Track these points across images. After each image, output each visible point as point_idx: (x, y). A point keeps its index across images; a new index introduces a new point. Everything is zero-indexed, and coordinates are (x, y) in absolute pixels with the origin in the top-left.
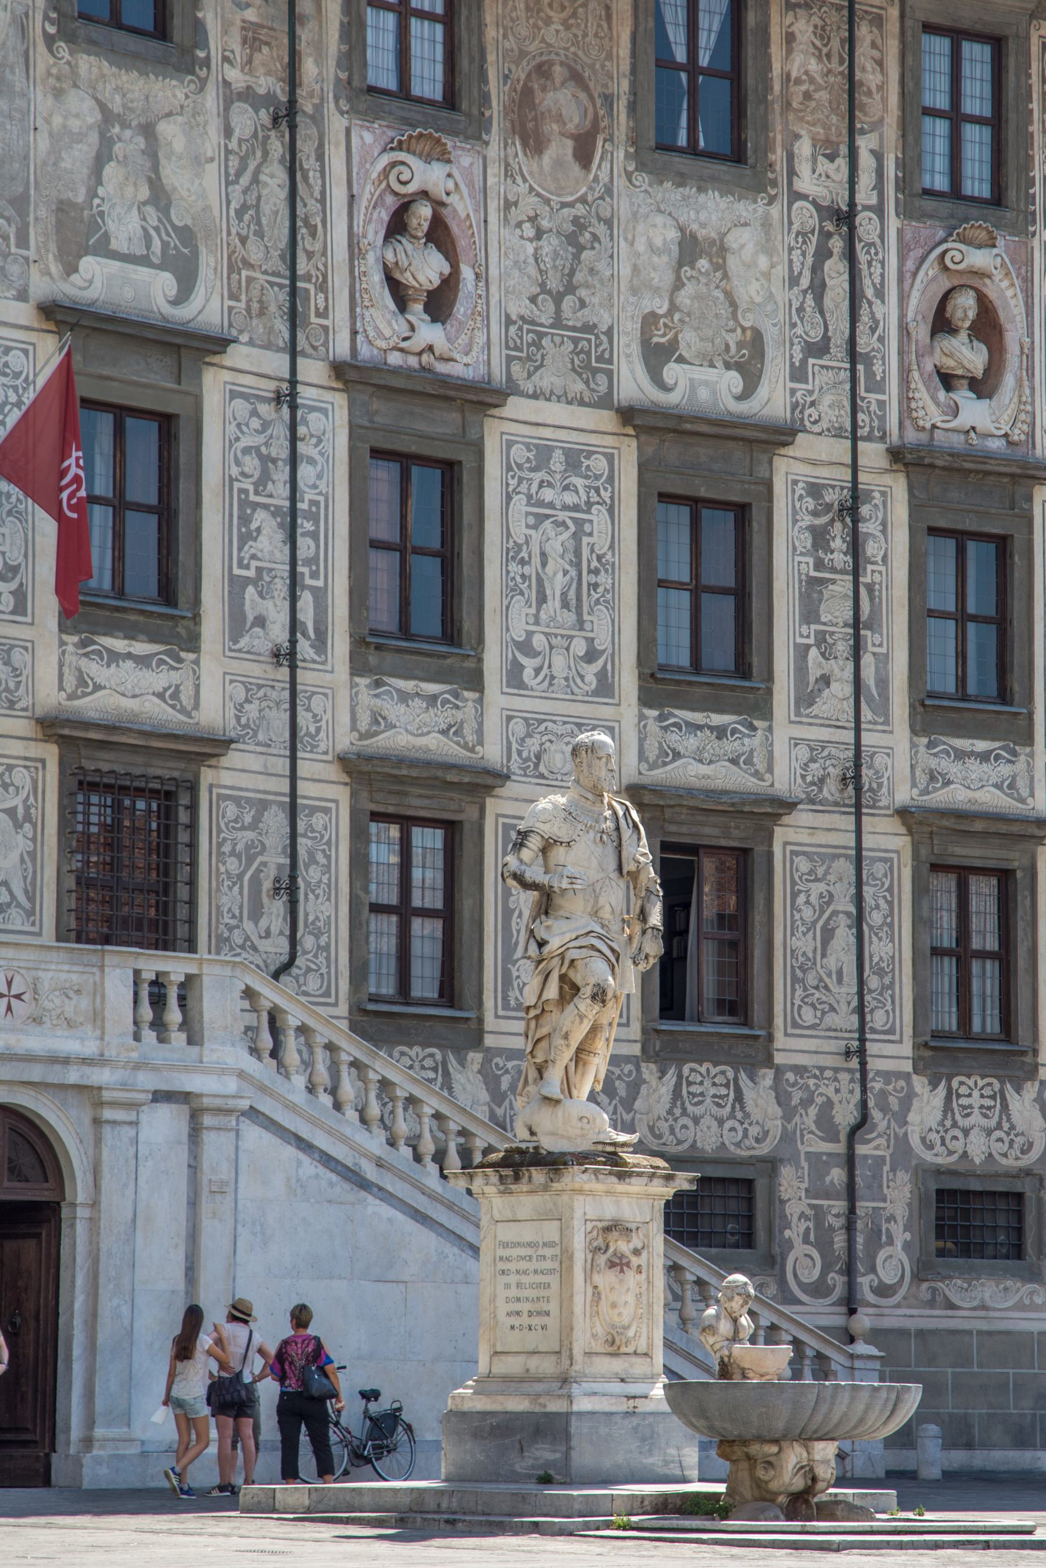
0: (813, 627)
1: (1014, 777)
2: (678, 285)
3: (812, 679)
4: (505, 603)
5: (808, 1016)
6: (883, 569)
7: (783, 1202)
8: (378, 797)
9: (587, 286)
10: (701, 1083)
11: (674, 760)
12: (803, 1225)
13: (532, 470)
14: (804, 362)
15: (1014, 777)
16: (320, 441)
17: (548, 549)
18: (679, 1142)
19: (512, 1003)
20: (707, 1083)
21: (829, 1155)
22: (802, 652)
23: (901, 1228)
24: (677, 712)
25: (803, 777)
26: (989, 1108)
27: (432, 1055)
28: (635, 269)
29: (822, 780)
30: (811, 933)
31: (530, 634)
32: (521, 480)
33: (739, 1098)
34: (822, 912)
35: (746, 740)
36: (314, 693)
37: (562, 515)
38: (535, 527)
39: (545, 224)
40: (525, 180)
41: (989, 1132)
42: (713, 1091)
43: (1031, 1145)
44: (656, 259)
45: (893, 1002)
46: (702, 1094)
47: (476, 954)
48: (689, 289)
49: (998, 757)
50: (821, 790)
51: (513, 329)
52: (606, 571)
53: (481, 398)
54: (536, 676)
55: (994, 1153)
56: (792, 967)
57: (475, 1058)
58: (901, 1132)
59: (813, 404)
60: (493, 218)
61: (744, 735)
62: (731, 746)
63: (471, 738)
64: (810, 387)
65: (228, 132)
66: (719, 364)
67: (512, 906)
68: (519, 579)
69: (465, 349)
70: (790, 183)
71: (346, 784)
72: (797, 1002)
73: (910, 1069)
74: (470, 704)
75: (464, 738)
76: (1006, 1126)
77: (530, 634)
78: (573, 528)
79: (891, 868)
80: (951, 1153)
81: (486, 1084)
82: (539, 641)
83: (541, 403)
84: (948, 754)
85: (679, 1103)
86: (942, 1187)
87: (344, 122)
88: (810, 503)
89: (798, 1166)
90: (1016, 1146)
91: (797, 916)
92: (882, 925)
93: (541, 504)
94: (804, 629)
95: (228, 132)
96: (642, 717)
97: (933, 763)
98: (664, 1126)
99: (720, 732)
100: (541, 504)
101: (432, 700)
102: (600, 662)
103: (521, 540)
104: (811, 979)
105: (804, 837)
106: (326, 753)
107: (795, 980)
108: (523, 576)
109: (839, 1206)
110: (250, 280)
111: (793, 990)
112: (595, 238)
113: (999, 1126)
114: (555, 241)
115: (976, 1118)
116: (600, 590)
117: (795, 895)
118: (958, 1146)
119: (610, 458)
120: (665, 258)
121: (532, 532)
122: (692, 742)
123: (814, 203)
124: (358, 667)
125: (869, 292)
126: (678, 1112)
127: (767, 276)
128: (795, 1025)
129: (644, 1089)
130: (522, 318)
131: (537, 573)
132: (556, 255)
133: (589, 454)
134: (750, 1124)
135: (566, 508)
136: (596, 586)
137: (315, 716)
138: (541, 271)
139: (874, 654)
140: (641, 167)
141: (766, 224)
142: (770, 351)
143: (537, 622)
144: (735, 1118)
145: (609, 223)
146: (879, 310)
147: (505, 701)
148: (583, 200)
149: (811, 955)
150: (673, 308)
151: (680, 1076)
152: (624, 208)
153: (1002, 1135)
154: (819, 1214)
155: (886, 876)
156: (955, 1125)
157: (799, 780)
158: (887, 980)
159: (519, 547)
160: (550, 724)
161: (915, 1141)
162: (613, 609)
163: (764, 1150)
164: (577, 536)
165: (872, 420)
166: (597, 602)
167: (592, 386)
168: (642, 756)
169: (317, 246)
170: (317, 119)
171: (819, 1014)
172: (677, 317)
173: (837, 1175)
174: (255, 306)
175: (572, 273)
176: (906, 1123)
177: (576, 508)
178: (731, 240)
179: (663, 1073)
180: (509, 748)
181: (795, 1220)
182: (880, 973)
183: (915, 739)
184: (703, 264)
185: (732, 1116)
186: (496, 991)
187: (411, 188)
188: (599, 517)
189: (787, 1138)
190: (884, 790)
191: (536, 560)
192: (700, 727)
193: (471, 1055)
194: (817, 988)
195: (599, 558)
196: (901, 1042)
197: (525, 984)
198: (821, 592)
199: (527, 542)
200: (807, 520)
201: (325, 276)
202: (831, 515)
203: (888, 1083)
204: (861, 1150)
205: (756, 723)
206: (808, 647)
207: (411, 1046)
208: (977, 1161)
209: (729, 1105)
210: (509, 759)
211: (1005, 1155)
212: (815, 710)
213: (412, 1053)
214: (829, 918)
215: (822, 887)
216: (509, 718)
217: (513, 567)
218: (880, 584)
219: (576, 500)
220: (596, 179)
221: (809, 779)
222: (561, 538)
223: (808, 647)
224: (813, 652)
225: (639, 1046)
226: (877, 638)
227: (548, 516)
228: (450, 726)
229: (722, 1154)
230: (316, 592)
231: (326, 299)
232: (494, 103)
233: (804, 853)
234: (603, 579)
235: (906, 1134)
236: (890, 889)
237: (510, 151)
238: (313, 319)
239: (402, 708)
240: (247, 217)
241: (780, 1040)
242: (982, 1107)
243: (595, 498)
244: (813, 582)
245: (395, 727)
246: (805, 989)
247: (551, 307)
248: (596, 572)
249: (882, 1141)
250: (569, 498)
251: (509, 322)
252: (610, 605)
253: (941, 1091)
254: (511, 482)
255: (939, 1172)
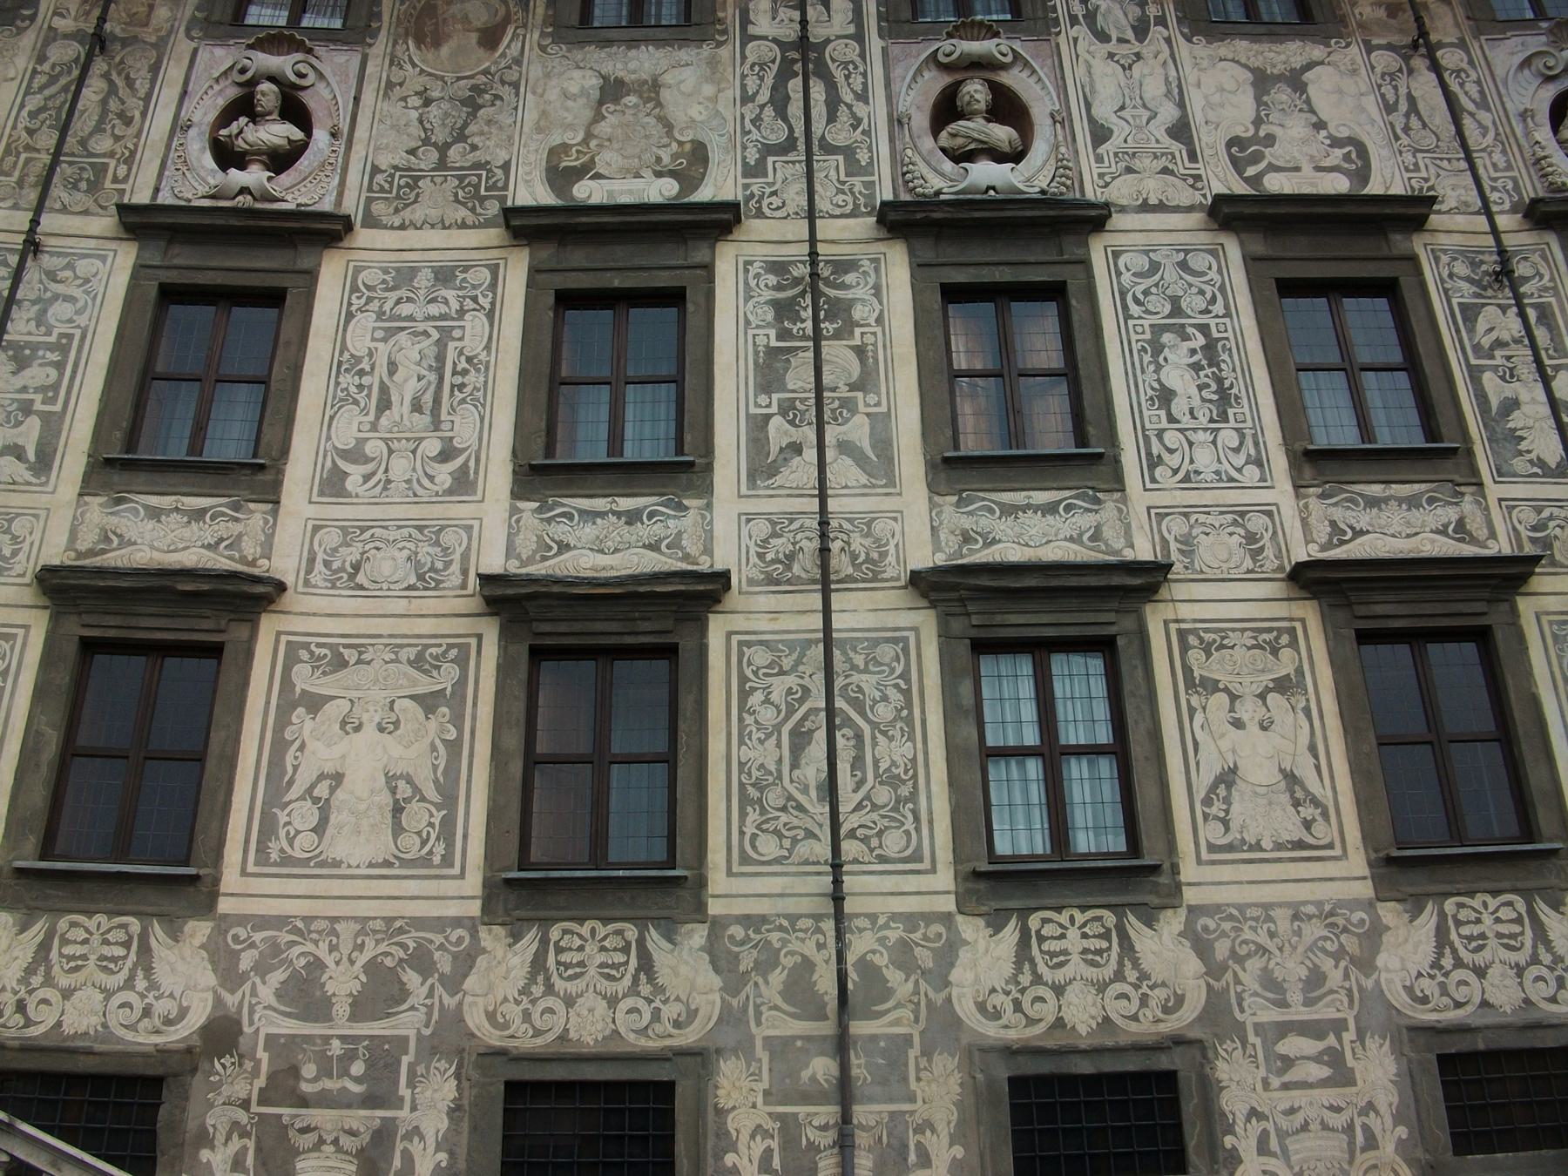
0: (775, 397)
1: (1098, 528)
2: (598, 117)
3: (774, 450)
4: (329, 413)
5: (769, 847)
6: (878, 330)
7: (721, 1113)
8: (87, 619)
9: (482, 133)
10: (581, 949)
11: (559, 553)
12: (759, 1147)
13: (387, 290)
14: (761, 162)
15: (1098, 528)
16: (87, 281)
17: (399, 358)
18: (538, 1033)
19: (274, 856)
20: (590, 948)
21: (807, 1038)
22: (759, 425)
23: (945, 1140)
24: (565, 501)
25: (761, 556)
26: (1099, 952)
27: (124, 926)
28: (544, 113)
29: (791, 557)
30: (773, 741)
31: (361, 442)
32: (369, 300)
33: (646, 964)
34: (791, 711)
35: (671, 523)
36: (18, 515)
37: (421, 327)
38: (385, 340)
39: (436, 94)
40: (414, 65)
41: (1101, 987)
42: (601, 958)
43: (1180, 1000)
44: (570, 103)
45: (917, 819)
46: (581, 964)
47: (221, 798)
48: (611, 119)
49: (1068, 508)
50: (789, 568)
51: (379, 178)
52: (478, 370)
53: (327, 231)
54: (365, 482)
55: (1114, 1016)
56: (742, 785)
57: (199, 930)
58: (939, 998)
59: (774, 193)
60: (368, 97)
61: (669, 516)
62: (647, 530)
63: (250, 549)
64: (770, 179)
65: (42, 59)
66: (648, 173)
67: (288, 736)
68: (353, 389)
69: (298, 191)
70: (743, 28)
71: (45, 607)
72: (750, 830)
73: (952, 907)
74: (258, 516)
75: (240, 551)
76: (1132, 975)
77: (361, 442)
78: (435, 335)
79: (906, 650)
80: (1031, 1022)
81: (212, 962)
82: (374, 448)
83: (410, 232)
84: (992, 511)
85: (540, 978)
86: (1019, 1072)
87: (194, 45)
88: (772, 280)
89: (750, 1056)
90: (1152, 1003)
91: (749, 720)
92: (895, 720)
93: (399, 318)
94: (763, 400)
95: (42, 59)
96: (514, 511)
97: (967, 523)
98: (513, 1012)
99: (632, 517)
100: (393, 318)
101: (199, 514)
102: (459, 461)
103: (363, 352)
104: (773, 798)
105: (763, 624)
106: (23, 575)
107: (745, 800)
108: (360, 387)
109: (828, 1113)
110: (28, 161)
111: (743, 815)
112: (497, 97)
113: (1119, 976)
114: (445, 106)
115: (1076, 967)
116: (468, 390)
117: (744, 695)
118: (1048, 1012)
119: (494, 270)
120: (582, 101)
121: (380, 345)
122: (589, 531)
123: (775, 41)
124: (89, 486)
125: (848, 97)
126: (538, 990)
127: (714, 99)
128: (745, 859)
129: (481, 961)
130: (396, 168)
131: (382, 382)
132: (446, 115)
133: (466, 269)
134: (665, 1002)
135: (429, 318)
136: (461, 387)
137: (14, 538)
138: (425, 130)
139: (868, 415)
140: (557, 39)
141: (713, 63)
142: (715, 155)
143: (374, 427)
144: (638, 994)
145: (516, 86)
146: (861, 110)
147: (312, 511)
148: (486, 72)
149: (773, 768)
150: (589, 135)
151: (545, 942)
152: (535, 71)
153: (1127, 988)
154: (789, 1129)
155: (898, 659)
156: (1038, 979)
157: (754, 559)
158: (905, 791)
159: (358, 360)
160: (378, 532)
161: (965, 1008)
162: (484, 406)
163: (688, 1038)
164: (441, 345)
165: (855, 198)
166: (463, 401)
167: (479, 210)
168: (510, 551)
169: (132, 130)
170: (161, 46)
171: (787, 843)
172: (593, 143)
173: (822, 1068)
174: (32, 179)
175: (465, 125)
176: (947, 984)
177: (443, 317)
178: (668, 78)
179: (516, 937)
180: (312, 560)
181: (744, 1137)
182: (893, 781)
183: (937, 498)
184: (631, 100)
185: (634, 990)
186: (247, 841)
187: (249, 75)
188: (475, 325)
189: (730, 1017)
190: (891, 558)
191: (382, 369)
192: (602, 515)
193: (191, 925)
194: (784, 809)
195: (469, 360)
196: (933, 870)
197: (298, 832)
198: (788, 361)
199: (370, 354)
200: (768, 295)
201: (133, 153)
202: (801, 288)
203: (914, 930)
204: (859, 1028)
205: (685, 502)
206: (768, 417)
207: (90, 914)
208: (1083, 1030)
209: (629, 977)
210: (309, 571)
211: (1135, 1018)
212: (778, 480)
213: (91, 923)
214: (804, 718)
215: (791, 681)
216: (316, 529)
217: (345, 379)
218: (875, 345)
219: (444, 309)
220: (504, 55)
221: (769, 557)
222: (418, 347)
223: (768, 417)
224: (776, 422)
225: (478, 903)
226: (872, 398)
227: (403, 329)
228: (222, 540)
229: (616, 1048)
230: (46, 418)
231: (130, 169)
232: (386, 18)
233: (761, 643)
234: (471, 378)
235: (949, 1000)
236: (905, 676)
237: (400, 49)
238: (108, 184)
239: (151, 524)
240: (42, 116)
241: (718, 881)
242: (1085, 951)
243: (469, 304)
244: (772, 352)
245: (135, 543)
246: (763, 811)
247: (434, 155)
248: (465, 372)
249: (906, 1013)
250: (434, 310)
251: (376, 170)
252: (479, 404)
253: (1010, 933)
254: (354, 301)
255: (1010, 1052)
